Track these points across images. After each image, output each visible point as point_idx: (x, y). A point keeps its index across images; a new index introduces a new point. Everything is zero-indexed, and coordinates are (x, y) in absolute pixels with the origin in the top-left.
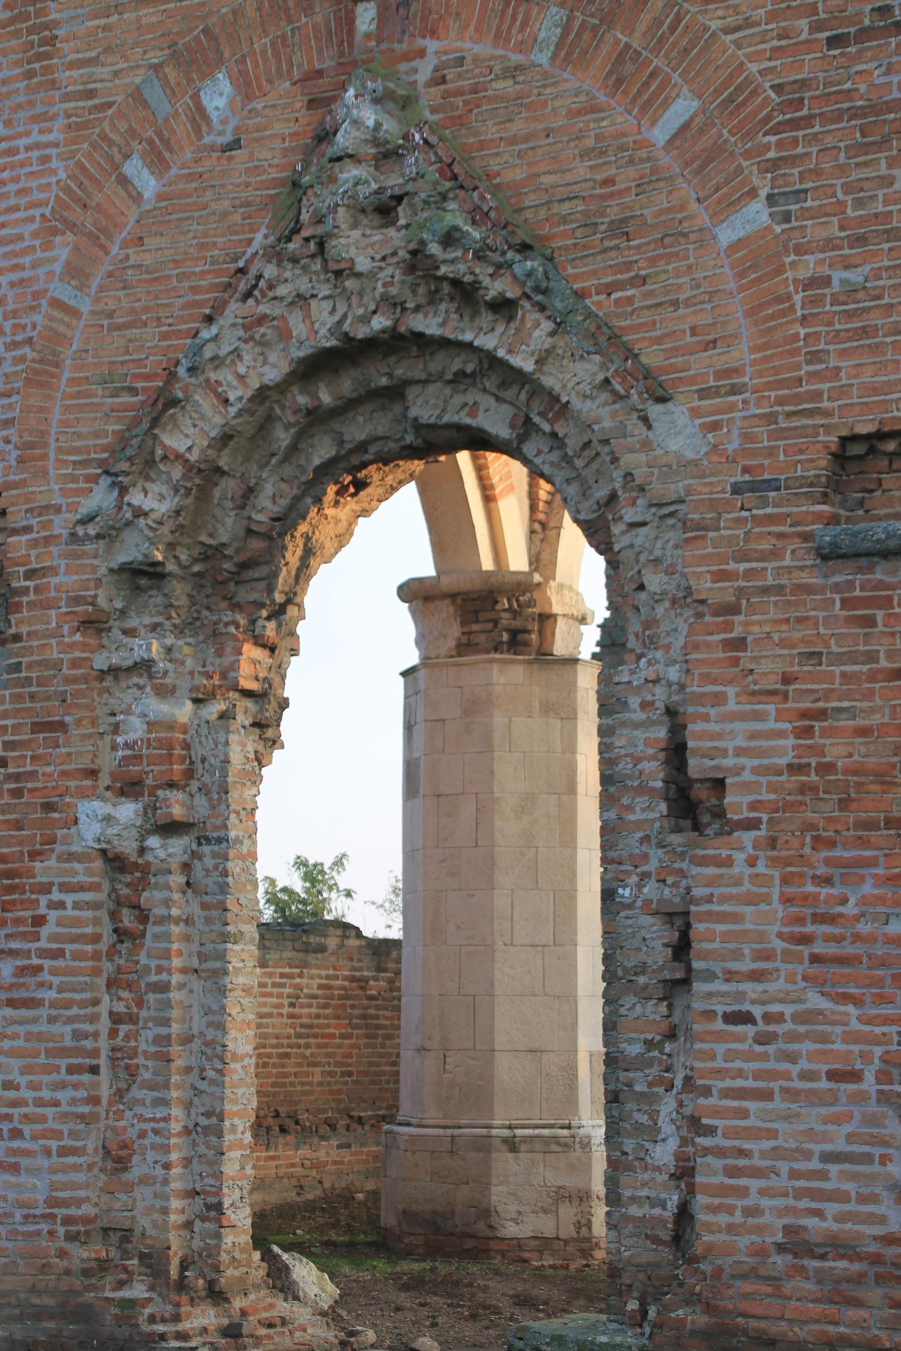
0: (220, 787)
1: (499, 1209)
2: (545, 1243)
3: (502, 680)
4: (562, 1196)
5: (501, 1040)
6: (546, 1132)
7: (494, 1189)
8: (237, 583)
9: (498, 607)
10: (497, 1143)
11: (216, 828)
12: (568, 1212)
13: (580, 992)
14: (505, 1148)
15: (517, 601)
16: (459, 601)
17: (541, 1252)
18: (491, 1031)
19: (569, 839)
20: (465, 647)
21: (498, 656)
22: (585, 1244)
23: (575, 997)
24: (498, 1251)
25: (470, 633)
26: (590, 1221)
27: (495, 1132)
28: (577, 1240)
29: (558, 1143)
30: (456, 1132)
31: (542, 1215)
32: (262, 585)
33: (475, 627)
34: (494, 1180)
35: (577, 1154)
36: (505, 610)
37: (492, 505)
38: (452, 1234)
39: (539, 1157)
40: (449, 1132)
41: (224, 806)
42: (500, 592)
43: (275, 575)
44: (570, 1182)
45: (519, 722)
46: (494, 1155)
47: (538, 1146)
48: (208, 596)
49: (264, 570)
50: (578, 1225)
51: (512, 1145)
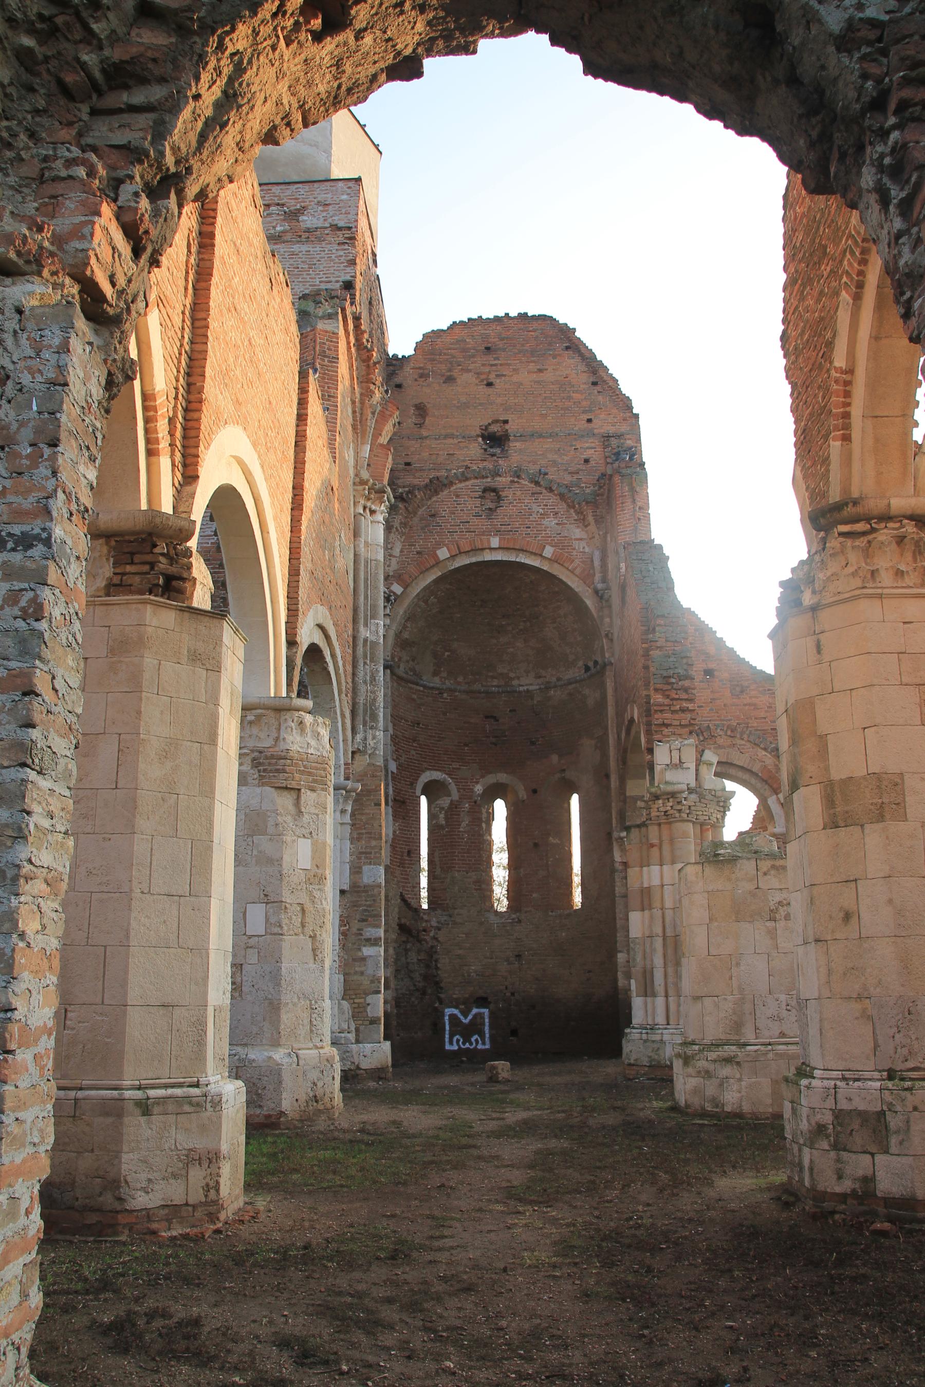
0: (38, 431)
1: (129, 1179)
2: (173, 1211)
3: (155, 622)
4: (192, 1158)
5: (134, 995)
6: (178, 1092)
7: (125, 1157)
8: (95, 112)
9: (156, 550)
10: (130, 1106)
11: (19, 515)
12: (197, 1175)
13: (212, 946)
14: (138, 1111)
15: (175, 548)
16: (113, 543)
17: (169, 1221)
18: (124, 984)
19: (208, 790)
20: (114, 587)
21: (152, 597)
22: (211, 1206)
23: (207, 950)
24: (124, 1226)
25: (123, 574)
26: (218, 1183)
27: (128, 1094)
28: (206, 1204)
29: (190, 1103)
30: (81, 1094)
31: (172, 1181)
32: (145, 120)
33: (129, 568)
34: (125, 1149)
35: (208, 1114)
36: (163, 554)
37: (153, 459)
38: (71, 1208)
39: (172, 1118)
40: (72, 1094)
41: (43, 470)
42: (160, 536)
43: (175, 109)
44: (200, 1143)
45: (168, 666)
46: (126, 1120)
47: (171, 1108)
48: (37, 112)
49: (156, 93)
50: (207, 1189)
51: (145, 1107)
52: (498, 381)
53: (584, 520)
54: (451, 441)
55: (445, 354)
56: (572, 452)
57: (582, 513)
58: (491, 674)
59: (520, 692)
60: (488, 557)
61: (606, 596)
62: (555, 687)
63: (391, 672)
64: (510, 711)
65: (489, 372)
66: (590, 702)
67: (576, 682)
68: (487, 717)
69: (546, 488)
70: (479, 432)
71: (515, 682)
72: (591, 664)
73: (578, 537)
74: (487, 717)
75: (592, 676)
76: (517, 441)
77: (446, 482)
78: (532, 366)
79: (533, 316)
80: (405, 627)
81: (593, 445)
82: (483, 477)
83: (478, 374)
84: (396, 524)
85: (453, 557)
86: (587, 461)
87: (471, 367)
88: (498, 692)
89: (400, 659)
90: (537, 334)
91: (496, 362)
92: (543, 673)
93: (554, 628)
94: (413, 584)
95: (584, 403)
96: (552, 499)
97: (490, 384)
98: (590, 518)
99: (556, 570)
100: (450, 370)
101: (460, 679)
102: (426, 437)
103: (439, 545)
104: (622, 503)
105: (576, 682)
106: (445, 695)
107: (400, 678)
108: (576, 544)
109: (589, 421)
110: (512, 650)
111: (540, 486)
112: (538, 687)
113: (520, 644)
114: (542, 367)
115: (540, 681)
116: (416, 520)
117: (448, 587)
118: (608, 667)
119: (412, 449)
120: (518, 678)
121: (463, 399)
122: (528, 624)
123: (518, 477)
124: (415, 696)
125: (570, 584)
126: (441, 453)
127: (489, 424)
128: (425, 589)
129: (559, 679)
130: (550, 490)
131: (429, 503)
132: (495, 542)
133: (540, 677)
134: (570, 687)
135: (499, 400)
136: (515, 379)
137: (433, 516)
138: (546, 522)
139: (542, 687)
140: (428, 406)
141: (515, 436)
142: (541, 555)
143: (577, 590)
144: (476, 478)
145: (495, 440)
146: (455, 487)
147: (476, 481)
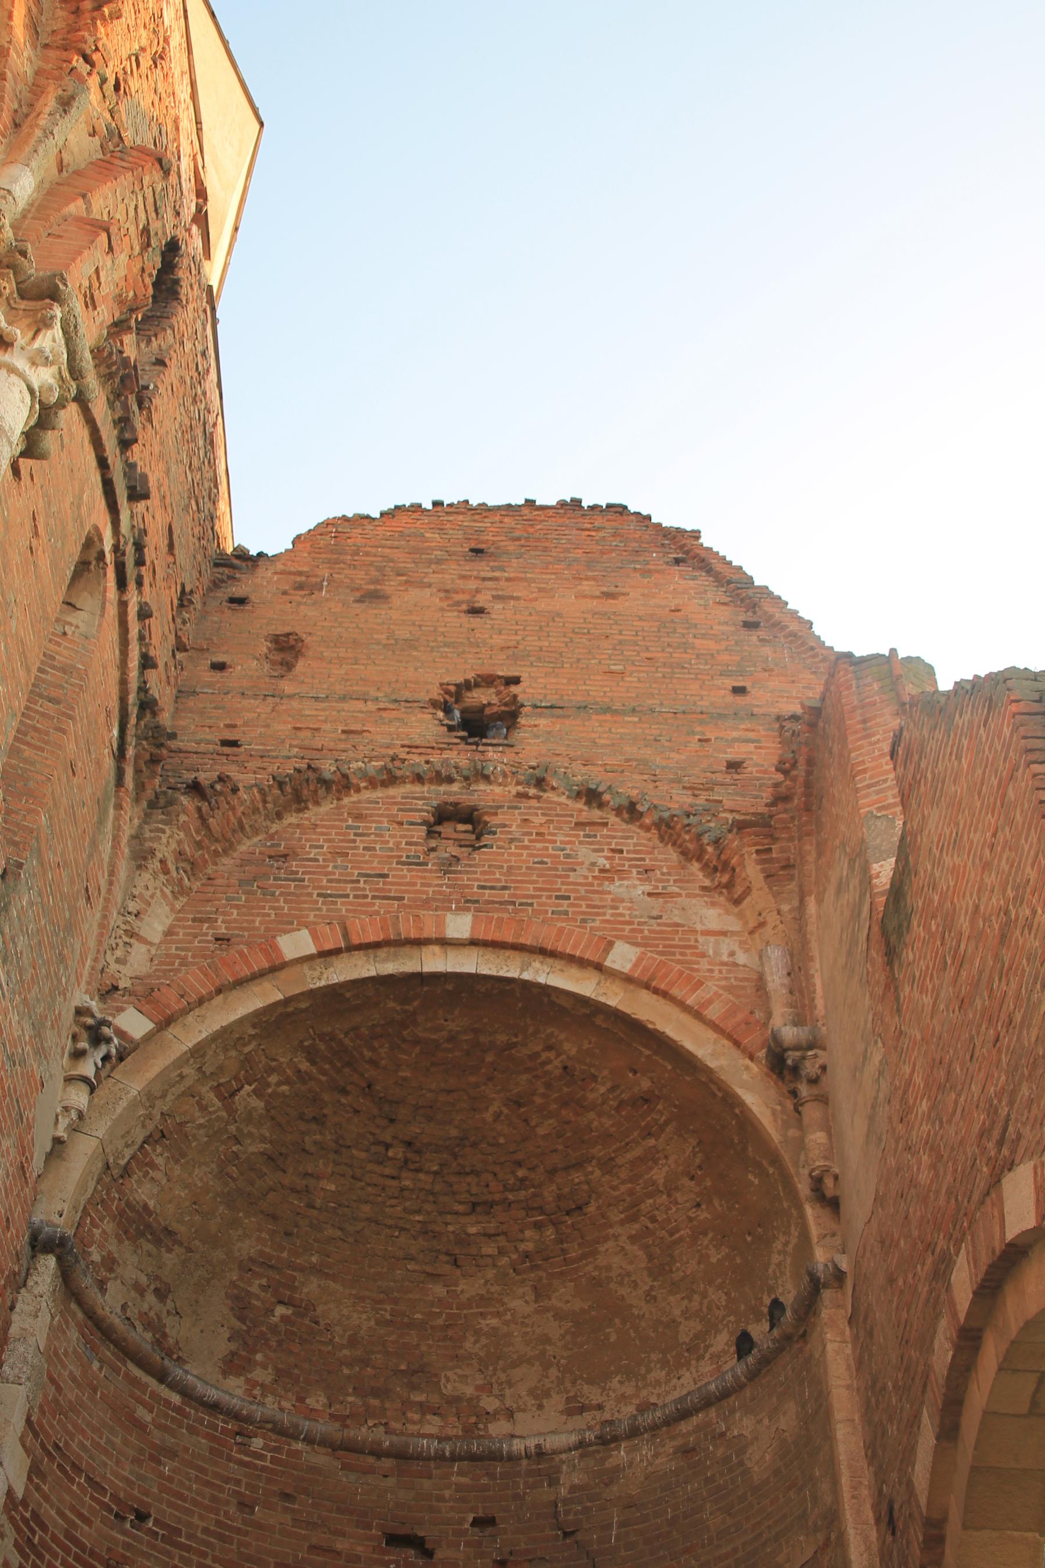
52: (499, 606)
53: (729, 886)
54: (360, 705)
55: (367, 554)
56: (694, 745)
57: (726, 864)
58: (418, 1397)
59: (512, 1458)
60: (435, 962)
61: (810, 1068)
62: (634, 1432)
63: (65, 1274)
64: (476, 1522)
65: (478, 591)
66: (760, 1459)
67: (708, 1402)
68: (395, 1540)
69: (618, 811)
70: (436, 694)
71: (498, 1428)
72: (759, 1330)
73: (715, 926)
74: (395, 1540)
75: (766, 1361)
76: (540, 715)
77: (327, 776)
78: (586, 586)
79: (594, 508)
80: (141, 1161)
81: (751, 735)
82: (442, 778)
83: (447, 591)
84: (166, 846)
85: (326, 955)
86: (734, 766)
87: (433, 578)
88: (440, 1457)
89: (110, 1263)
90: (602, 534)
91: (497, 574)
92: (592, 1394)
93: (633, 1239)
94: (190, 1018)
95: (725, 657)
96: (635, 839)
97: (476, 611)
98: (752, 871)
99: (646, 1009)
100: (376, 582)
101: (317, 1401)
102: (291, 697)
103: (287, 924)
104: (864, 721)
105: (708, 1402)
106: (257, 1443)
107: (97, 1326)
108: (708, 944)
109: (739, 691)
110: (494, 1322)
111: (601, 806)
112: (573, 1439)
113: (520, 1303)
114: (612, 589)
115: (580, 1421)
116: (227, 862)
117: (304, 1066)
118: (827, 1294)
119: (248, 716)
120: (510, 1414)
121: (403, 633)
122: (550, 1233)
123: (540, 783)
124: (144, 1415)
125: (689, 1045)
126: (328, 727)
127: (468, 686)
128: (223, 1037)
129: (644, 1407)
130: (631, 811)
131: (275, 827)
132: (459, 925)
133: (582, 1409)
134: (684, 1427)
135: (498, 640)
136: (542, 605)
137: (285, 856)
138: (617, 888)
139: (589, 1436)
140: (308, 640)
141: (535, 707)
142: (599, 967)
143: (712, 1064)
144: (419, 779)
145: (479, 718)
146: (355, 797)
147: (417, 789)
